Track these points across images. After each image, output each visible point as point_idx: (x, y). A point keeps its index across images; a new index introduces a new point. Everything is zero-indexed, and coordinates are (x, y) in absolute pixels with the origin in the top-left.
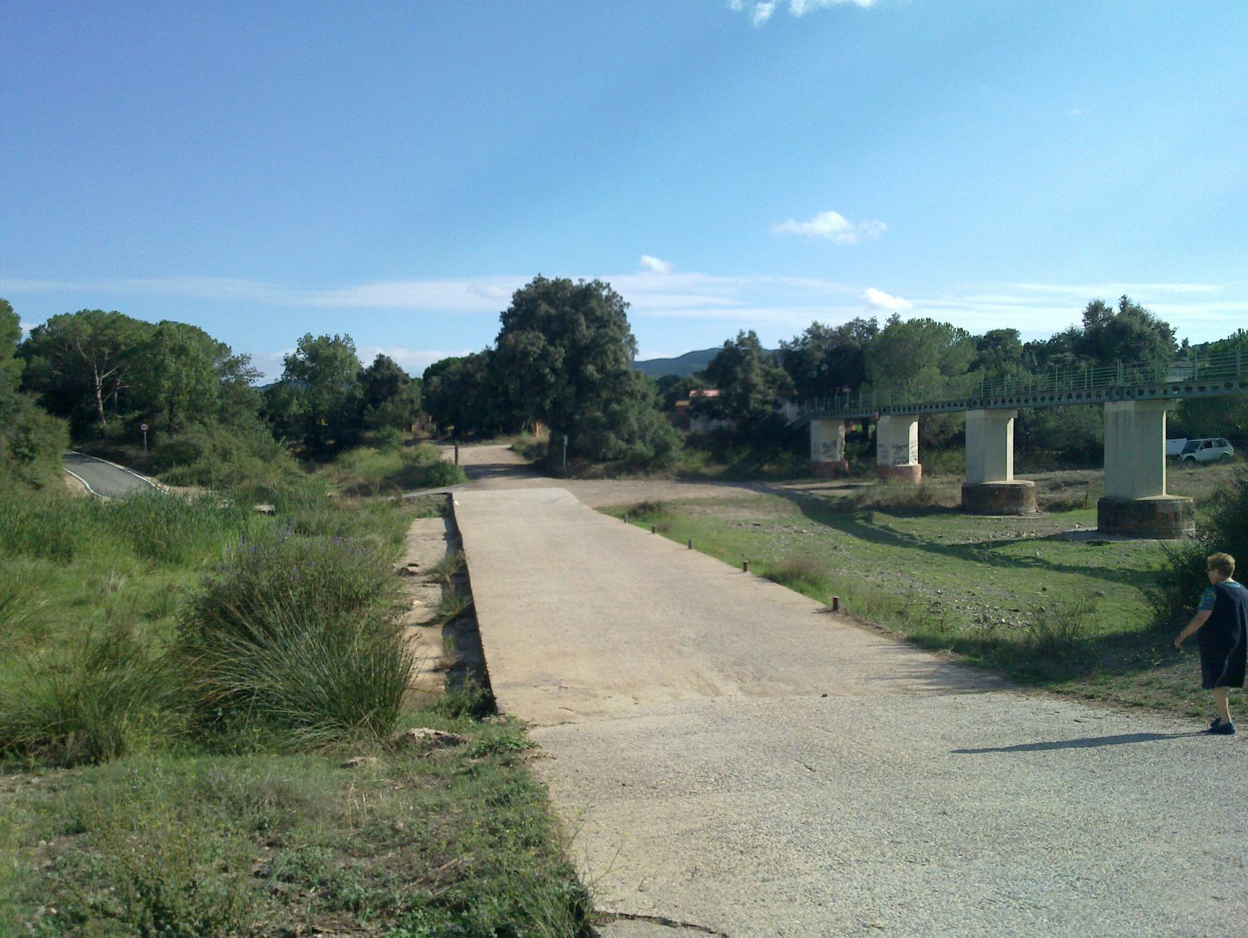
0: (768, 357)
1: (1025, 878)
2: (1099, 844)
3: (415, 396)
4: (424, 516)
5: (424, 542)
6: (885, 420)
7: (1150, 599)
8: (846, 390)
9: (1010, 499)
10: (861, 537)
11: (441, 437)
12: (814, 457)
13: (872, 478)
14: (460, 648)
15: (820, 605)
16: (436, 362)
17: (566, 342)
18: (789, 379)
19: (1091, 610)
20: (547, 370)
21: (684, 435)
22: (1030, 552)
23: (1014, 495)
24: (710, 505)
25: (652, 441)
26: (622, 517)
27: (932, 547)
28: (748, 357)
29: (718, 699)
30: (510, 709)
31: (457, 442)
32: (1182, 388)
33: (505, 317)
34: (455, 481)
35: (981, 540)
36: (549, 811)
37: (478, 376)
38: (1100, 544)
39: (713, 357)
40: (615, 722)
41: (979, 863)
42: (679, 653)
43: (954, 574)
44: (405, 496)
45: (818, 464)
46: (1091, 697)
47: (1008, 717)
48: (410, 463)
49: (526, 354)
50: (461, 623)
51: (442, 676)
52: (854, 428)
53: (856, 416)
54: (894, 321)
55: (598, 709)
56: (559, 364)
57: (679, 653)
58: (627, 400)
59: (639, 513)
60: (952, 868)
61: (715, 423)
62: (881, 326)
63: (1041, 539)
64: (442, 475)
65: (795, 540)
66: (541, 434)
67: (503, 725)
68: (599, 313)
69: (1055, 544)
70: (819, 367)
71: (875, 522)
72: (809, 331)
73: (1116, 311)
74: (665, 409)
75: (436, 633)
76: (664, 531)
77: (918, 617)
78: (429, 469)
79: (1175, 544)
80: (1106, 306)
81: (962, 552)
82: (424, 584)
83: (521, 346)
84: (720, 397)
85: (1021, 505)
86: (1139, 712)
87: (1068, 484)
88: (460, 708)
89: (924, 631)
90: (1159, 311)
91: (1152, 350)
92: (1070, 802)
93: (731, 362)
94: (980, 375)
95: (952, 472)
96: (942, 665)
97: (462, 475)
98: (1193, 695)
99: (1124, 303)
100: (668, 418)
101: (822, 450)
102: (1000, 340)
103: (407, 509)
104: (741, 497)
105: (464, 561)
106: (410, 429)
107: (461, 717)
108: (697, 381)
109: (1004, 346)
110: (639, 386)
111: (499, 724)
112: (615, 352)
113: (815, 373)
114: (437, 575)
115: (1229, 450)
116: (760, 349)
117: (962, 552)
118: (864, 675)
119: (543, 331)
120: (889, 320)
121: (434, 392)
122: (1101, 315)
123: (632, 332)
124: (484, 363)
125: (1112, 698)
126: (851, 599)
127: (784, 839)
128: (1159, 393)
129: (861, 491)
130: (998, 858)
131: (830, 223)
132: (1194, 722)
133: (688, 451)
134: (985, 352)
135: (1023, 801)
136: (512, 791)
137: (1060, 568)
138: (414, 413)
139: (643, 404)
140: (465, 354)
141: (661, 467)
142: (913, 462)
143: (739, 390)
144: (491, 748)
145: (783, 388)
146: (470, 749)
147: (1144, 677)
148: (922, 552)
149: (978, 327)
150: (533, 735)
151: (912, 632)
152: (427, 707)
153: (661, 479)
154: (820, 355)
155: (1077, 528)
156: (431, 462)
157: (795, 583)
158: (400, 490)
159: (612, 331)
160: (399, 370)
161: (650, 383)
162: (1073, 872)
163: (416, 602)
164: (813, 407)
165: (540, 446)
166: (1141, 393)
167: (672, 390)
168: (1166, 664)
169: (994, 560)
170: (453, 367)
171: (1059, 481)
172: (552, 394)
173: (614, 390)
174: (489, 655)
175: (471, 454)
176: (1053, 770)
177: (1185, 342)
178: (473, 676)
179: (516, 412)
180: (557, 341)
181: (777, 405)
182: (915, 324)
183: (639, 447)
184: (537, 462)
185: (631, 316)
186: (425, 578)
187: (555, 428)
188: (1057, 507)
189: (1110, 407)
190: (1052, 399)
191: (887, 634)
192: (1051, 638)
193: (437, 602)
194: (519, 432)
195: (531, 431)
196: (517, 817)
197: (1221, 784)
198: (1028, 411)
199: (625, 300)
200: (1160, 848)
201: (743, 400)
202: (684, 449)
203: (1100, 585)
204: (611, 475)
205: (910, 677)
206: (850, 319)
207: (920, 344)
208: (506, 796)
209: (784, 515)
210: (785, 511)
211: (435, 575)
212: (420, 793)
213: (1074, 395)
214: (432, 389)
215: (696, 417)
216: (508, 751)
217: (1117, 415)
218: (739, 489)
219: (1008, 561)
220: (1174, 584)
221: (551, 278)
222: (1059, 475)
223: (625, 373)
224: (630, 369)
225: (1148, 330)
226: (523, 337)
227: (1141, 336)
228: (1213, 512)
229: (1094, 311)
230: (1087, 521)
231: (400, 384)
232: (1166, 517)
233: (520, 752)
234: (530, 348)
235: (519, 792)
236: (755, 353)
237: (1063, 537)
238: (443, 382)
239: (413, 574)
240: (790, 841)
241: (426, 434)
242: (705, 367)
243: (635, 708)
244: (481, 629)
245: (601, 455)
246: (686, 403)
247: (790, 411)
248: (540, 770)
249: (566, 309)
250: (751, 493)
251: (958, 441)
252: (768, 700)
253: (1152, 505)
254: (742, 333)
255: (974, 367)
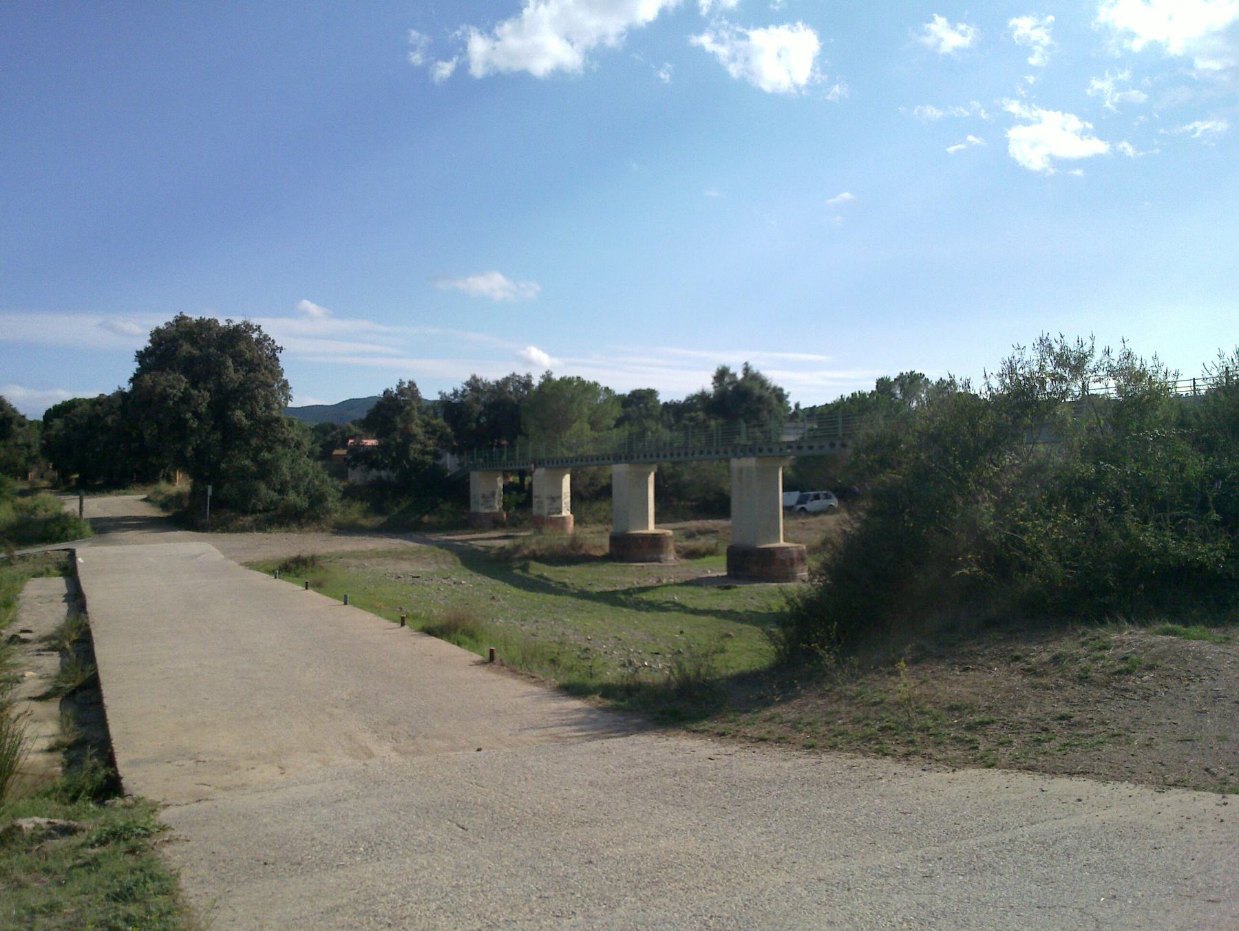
0: (428, 408)
1: (664, 921)
2: (729, 880)
3: (32, 440)
4: (40, 575)
5: (41, 605)
6: (540, 472)
7: (771, 640)
8: (504, 442)
9: (650, 548)
10: (517, 586)
11: (63, 486)
12: (473, 508)
13: (527, 529)
14: (81, 723)
15: (477, 657)
16: (59, 403)
17: (211, 385)
18: (449, 430)
19: (723, 651)
20: (189, 415)
21: (341, 485)
22: (669, 597)
23: (655, 543)
24: (368, 558)
25: (306, 493)
26: (272, 572)
27: (584, 595)
28: (408, 407)
29: (370, 762)
30: (138, 789)
31: (82, 492)
32: (795, 446)
33: (141, 356)
34: (79, 536)
35: (627, 586)
36: (179, 901)
37: (109, 420)
38: (728, 588)
39: (372, 406)
40: (259, 796)
41: (621, 911)
42: (331, 715)
43: (603, 620)
44: (17, 553)
45: (477, 515)
46: (723, 735)
47: (650, 759)
48: (26, 514)
49: (164, 397)
50: (82, 696)
51: (59, 756)
52: (511, 479)
53: (513, 467)
54: (548, 378)
55: (240, 783)
56: (203, 409)
57: (331, 715)
58: (279, 448)
59: (290, 568)
60: (596, 918)
61: (374, 473)
62: (536, 382)
63: (679, 585)
64: (64, 529)
65: (454, 591)
66: (181, 484)
67: (129, 807)
68: (248, 356)
69: (691, 589)
70: (478, 419)
71: (530, 571)
72: (468, 384)
73: (740, 376)
74: (321, 458)
75: (53, 707)
76: (318, 586)
77: (569, 664)
78: (47, 522)
79: (791, 586)
80: (731, 371)
81: (611, 598)
82: (39, 652)
83: (159, 389)
84: (379, 446)
85: (661, 552)
86: (763, 746)
87: (703, 532)
88: (79, 792)
89: (575, 677)
90: (775, 377)
91: (770, 411)
92: (704, 841)
93: (391, 410)
94: (625, 431)
95: (600, 522)
96: (590, 711)
97: (88, 529)
98: (809, 729)
99: (747, 369)
100: (324, 467)
101: (481, 501)
102: (643, 398)
103: (20, 567)
104: (400, 548)
105: (87, 625)
106: (26, 478)
107: (80, 802)
108: (355, 430)
109: (646, 405)
110: (293, 434)
111: (125, 807)
112: (266, 398)
113: (474, 425)
114: (54, 642)
115: (834, 502)
116: (420, 400)
117: (611, 598)
118: (517, 726)
119: (185, 372)
120: (543, 377)
121: (56, 436)
122: (727, 379)
123: (285, 377)
124: (116, 405)
125: (741, 734)
126: (506, 650)
127: (433, 906)
128: (776, 449)
129: (518, 541)
130: (639, 904)
131: (492, 284)
132: (809, 753)
133: (345, 502)
134: (629, 409)
135: (663, 843)
136: (136, 884)
137: (695, 612)
138: (32, 459)
139: (298, 453)
140: (93, 394)
141: (316, 518)
142: (566, 513)
143: (399, 440)
144: (115, 835)
145: (442, 438)
146: (89, 838)
147: (767, 713)
148: (573, 600)
149: (623, 385)
150: (163, 816)
151: (563, 680)
152: (38, 793)
153: (316, 531)
154: (479, 408)
155: (710, 574)
156: (50, 513)
157: (453, 636)
158: (12, 547)
159: (262, 376)
160: (14, 410)
161: (305, 431)
162: (707, 910)
163: (28, 674)
164: (472, 458)
165: (179, 496)
166: (761, 450)
167: (329, 438)
168: (786, 700)
169: (640, 606)
170: (79, 409)
171: (694, 529)
172: (195, 441)
173: (265, 437)
174: (115, 729)
175: (98, 506)
176: (690, 809)
177: (797, 406)
178: (96, 755)
179: (153, 460)
180: (201, 385)
181: (437, 456)
182: (566, 382)
183: (292, 497)
184: (175, 514)
185: (284, 360)
186: (40, 646)
187: (197, 477)
188: (692, 554)
189: (735, 463)
190: (686, 454)
191: (539, 683)
192: (688, 679)
193: (53, 673)
194: (156, 481)
195: (170, 480)
196: (142, 912)
197: (833, 811)
198: (666, 465)
199: (278, 344)
200: (780, 879)
201: (403, 449)
202: (341, 499)
203: (730, 626)
204: (260, 528)
205: (562, 725)
206: (506, 374)
207: (572, 401)
208: (129, 889)
209: (444, 567)
210: (445, 562)
211: (52, 643)
212: (25, 893)
213: (705, 451)
214: (53, 433)
215: (354, 467)
216: (132, 838)
217: (741, 470)
218: (399, 541)
219: (652, 606)
220: (791, 625)
221: (195, 317)
222: (693, 524)
223: (278, 420)
224: (283, 416)
225: (766, 394)
226: (162, 378)
227: (760, 399)
228: (822, 558)
229: (722, 374)
230: (717, 567)
231: (14, 427)
232: (783, 562)
233: (149, 836)
234: (169, 390)
235: (145, 882)
236: (414, 404)
237: (698, 582)
238: (66, 425)
239: (25, 641)
240: (440, 908)
241: (45, 483)
242: (363, 416)
243: (282, 778)
244: (106, 701)
245: (250, 506)
246: (343, 452)
247: (450, 462)
248: (171, 856)
249: (212, 350)
250: (411, 544)
251: (606, 492)
252: (422, 759)
253: (771, 552)
254: (401, 383)
255: (619, 423)
